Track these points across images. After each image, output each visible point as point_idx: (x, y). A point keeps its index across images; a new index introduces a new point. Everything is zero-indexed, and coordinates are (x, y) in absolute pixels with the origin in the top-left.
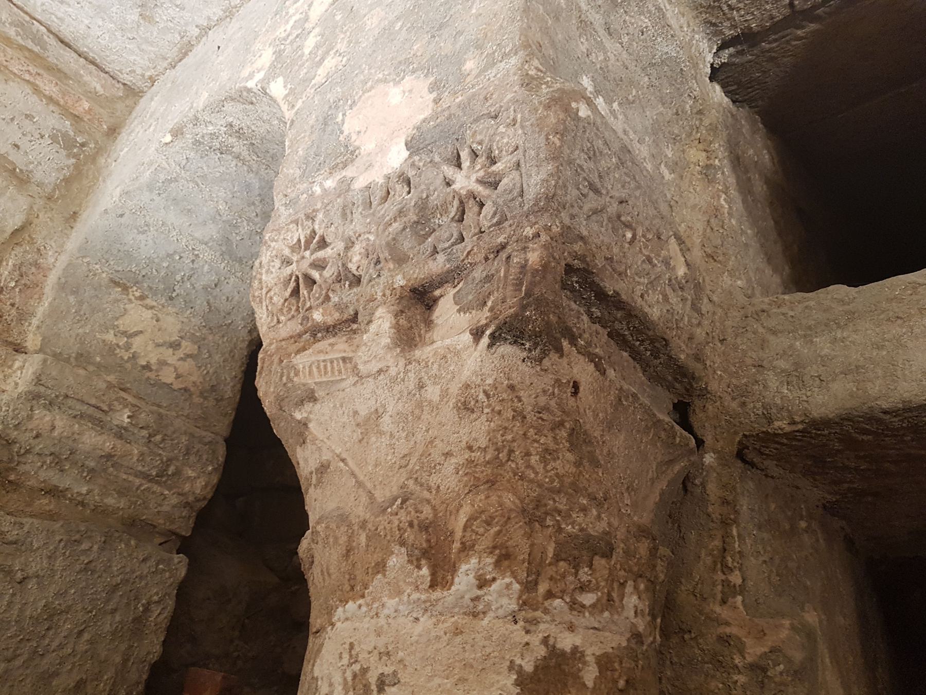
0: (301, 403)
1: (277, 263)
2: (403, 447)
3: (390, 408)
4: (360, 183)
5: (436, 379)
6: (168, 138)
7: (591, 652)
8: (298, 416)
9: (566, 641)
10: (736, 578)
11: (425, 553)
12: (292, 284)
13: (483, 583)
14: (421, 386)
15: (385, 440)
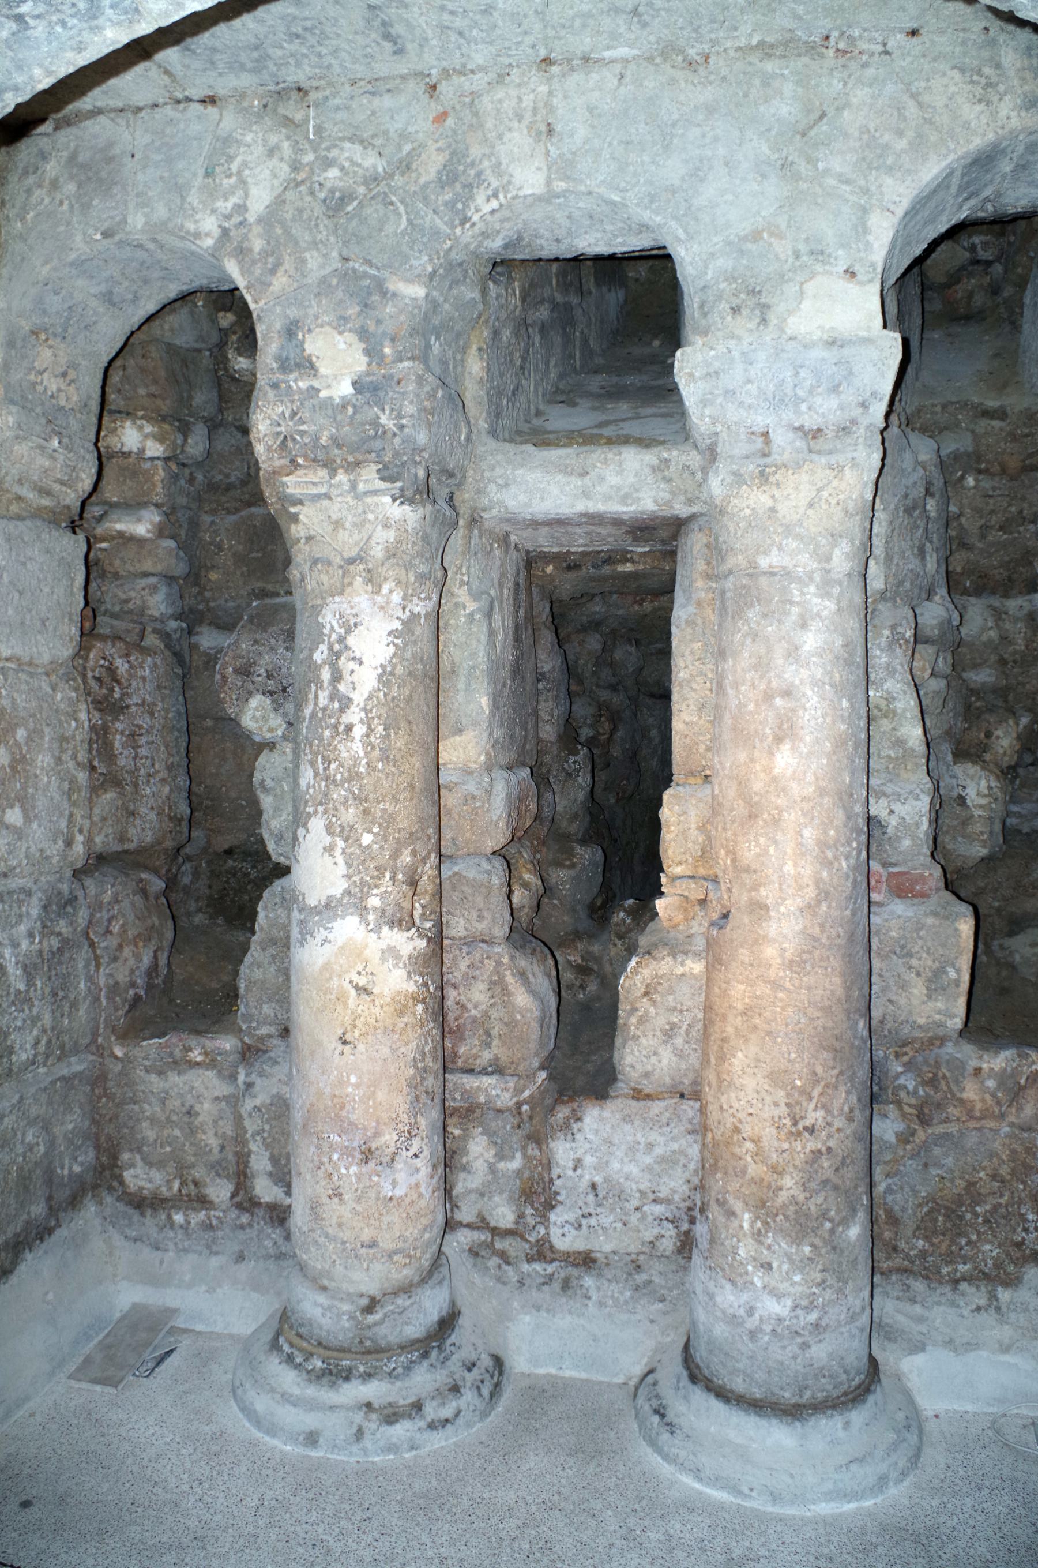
0: (294, 504)
1: (268, 422)
2: (356, 537)
3: (350, 518)
4: (323, 394)
5: (373, 512)
6: (98, 237)
7: (423, 613)
8: (292, 510)
9: (416, 610)
10: (466, 578)
11: (370, 580)
12: (282, 438)
13: (391, 592)
14: (365, 512)
15: (347, 533)
